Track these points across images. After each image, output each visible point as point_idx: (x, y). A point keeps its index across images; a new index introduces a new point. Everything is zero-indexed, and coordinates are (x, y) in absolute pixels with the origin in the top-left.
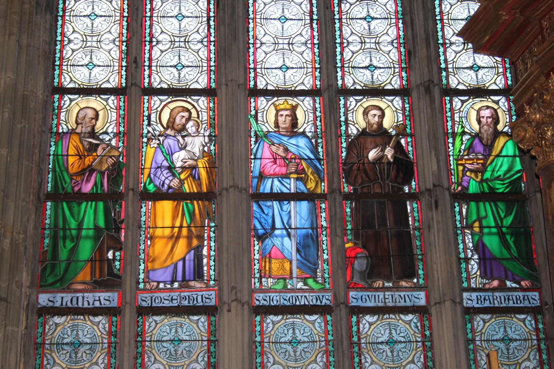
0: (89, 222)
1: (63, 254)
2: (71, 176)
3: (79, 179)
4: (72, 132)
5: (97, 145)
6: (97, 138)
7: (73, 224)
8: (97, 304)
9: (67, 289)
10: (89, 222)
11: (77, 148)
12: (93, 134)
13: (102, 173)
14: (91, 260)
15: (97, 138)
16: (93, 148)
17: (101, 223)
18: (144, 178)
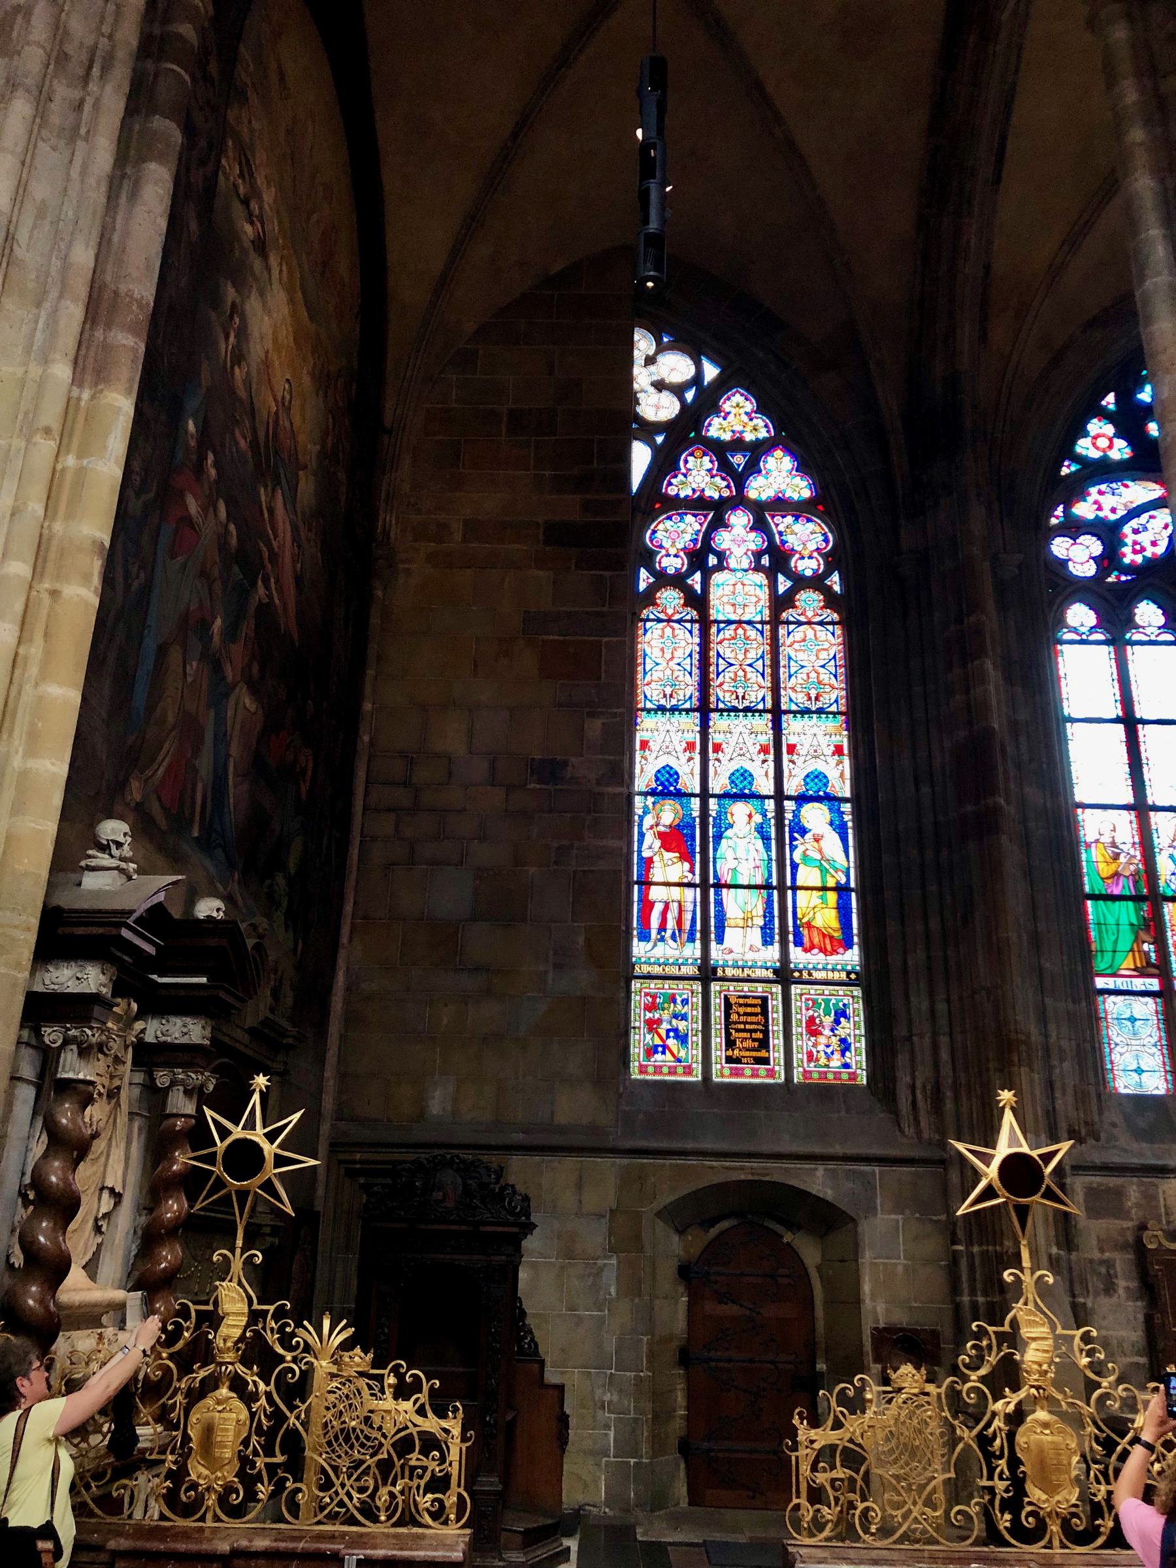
0: (1124, 920)
1: (1108, 946)
2: (1103, 879)
3: (1109, 881)
4: (1097, 841)
5: (1119, 854)
6: (1117, 847)
7: (1111, 920)
8: (1143, 988)
9: (1114, 975)
10: (1124, 920)
11: (1103, 856)
12: (1114, 844)
13: (1127, 877)
14: (1132, 950)
15: (1117, 847)
16: (1116, 857)
17: (1135, 921)
18: (1161, 883)
